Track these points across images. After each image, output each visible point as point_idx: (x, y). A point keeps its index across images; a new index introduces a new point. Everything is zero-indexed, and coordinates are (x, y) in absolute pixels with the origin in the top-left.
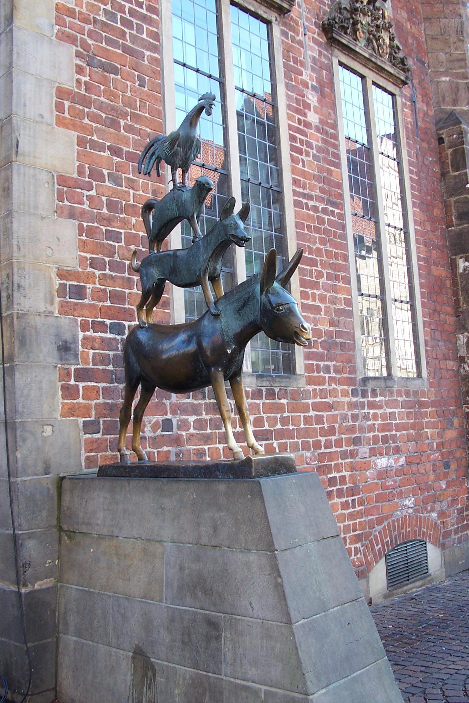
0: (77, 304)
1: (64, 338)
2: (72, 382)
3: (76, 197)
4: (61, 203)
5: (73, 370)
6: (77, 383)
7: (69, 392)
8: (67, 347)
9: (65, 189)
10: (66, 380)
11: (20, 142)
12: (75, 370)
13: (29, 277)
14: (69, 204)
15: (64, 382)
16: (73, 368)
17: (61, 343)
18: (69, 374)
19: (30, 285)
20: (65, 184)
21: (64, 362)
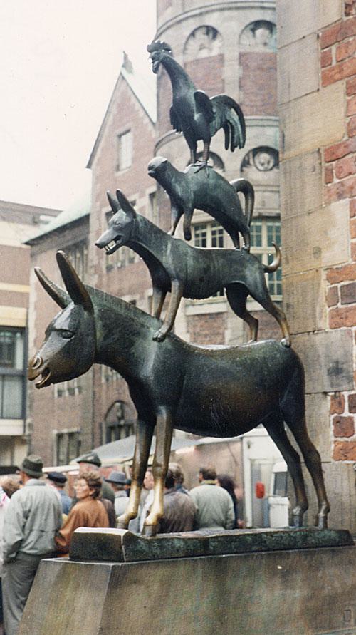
0: (348, 310)
1: (334, 358)
2: (346, 414)
3: (345, 168)
4: (329, 185)
5: (346, 399)
6: (352, 415)
7: (343, 427)
8: (337, 368)
9: (334, 163)
10: (338, 411)
11: (286, 134)
12: (350, 396)
13: (297, 291)
14: (338, 181)
15: (336, 415)
16: (346, 394)
17: (331, 365)
18: (341, 404)
19: (298, 302)
20: (334, 157)
21: (335, 390)
